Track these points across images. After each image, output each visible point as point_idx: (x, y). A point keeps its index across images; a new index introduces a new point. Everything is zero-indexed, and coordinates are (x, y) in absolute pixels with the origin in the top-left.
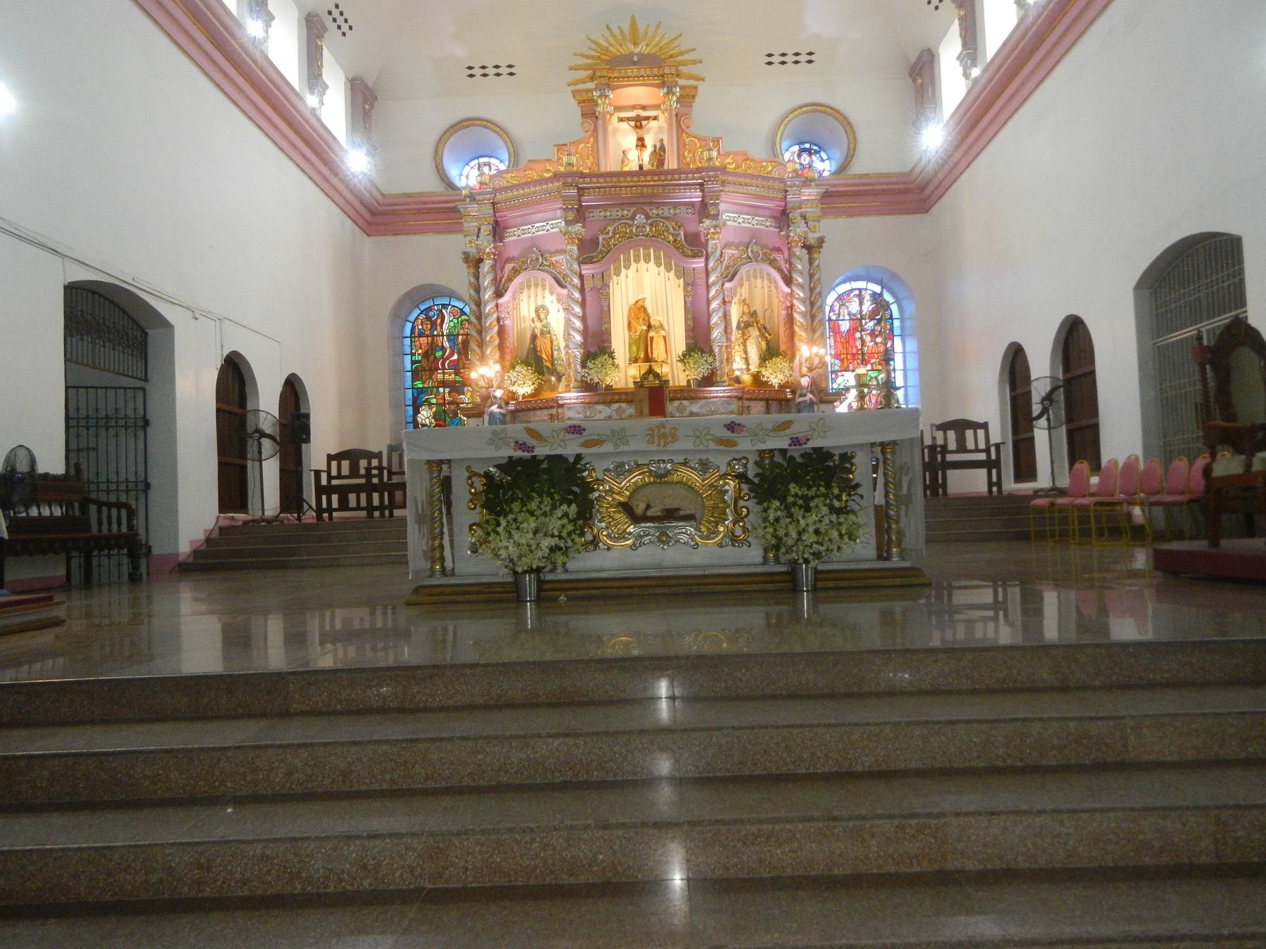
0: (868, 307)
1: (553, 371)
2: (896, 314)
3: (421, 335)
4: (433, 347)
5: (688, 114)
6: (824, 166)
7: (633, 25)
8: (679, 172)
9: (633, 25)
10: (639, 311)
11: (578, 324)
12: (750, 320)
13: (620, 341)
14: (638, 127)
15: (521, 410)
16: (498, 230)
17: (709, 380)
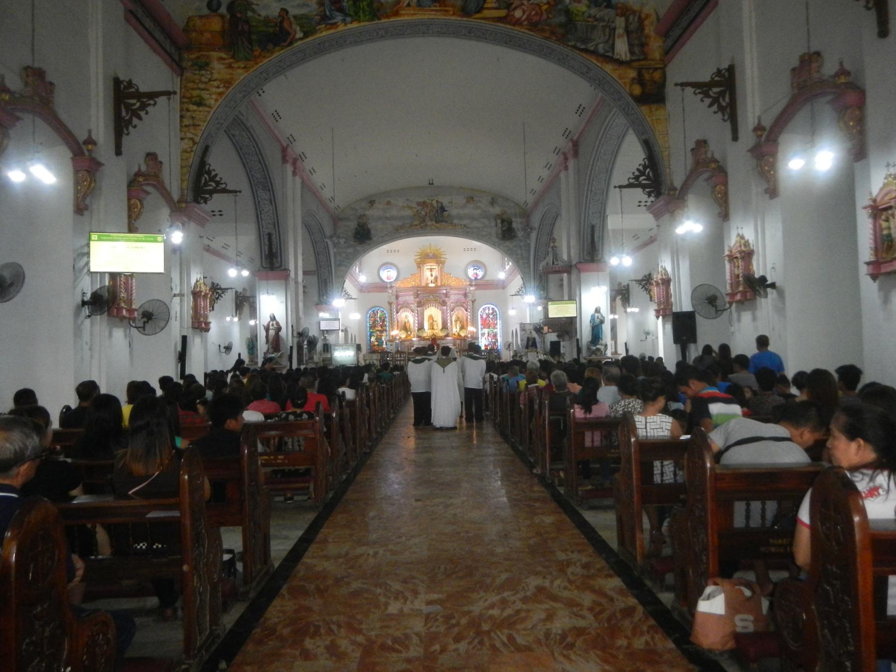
0: (491, 311)
1: (410, 331)
2: (498, 313)
3: (372, 317)
4: (375, 321)
5: (443, 268)
6: (480, 273)
7: (430, 245)
8: (441, 286)
9: (430, 245)
10: (431, 317)
11: (417, 322)
12: (458, 319)
13: (426, 326)
14: (431, 271)
15: (402, 341)
16: (397, 297)
17: (447, 336)
